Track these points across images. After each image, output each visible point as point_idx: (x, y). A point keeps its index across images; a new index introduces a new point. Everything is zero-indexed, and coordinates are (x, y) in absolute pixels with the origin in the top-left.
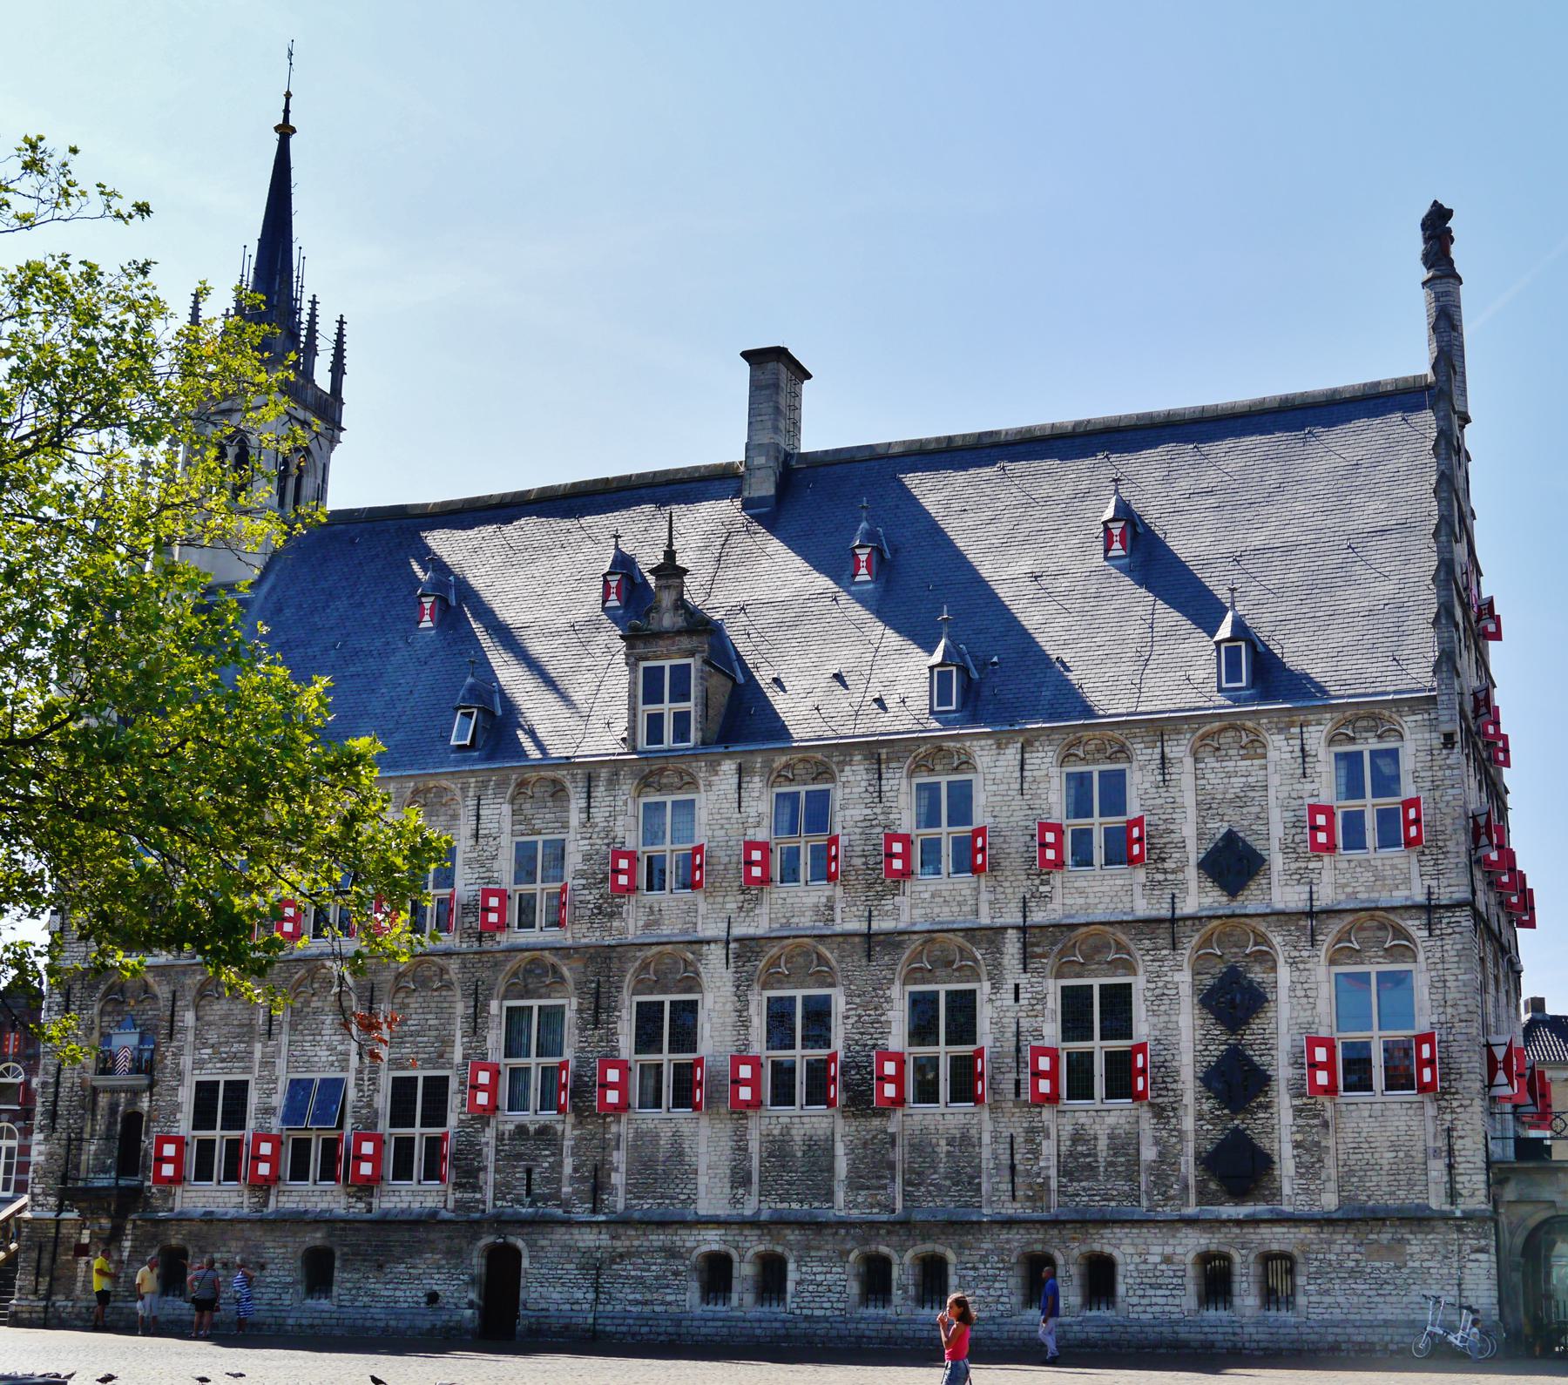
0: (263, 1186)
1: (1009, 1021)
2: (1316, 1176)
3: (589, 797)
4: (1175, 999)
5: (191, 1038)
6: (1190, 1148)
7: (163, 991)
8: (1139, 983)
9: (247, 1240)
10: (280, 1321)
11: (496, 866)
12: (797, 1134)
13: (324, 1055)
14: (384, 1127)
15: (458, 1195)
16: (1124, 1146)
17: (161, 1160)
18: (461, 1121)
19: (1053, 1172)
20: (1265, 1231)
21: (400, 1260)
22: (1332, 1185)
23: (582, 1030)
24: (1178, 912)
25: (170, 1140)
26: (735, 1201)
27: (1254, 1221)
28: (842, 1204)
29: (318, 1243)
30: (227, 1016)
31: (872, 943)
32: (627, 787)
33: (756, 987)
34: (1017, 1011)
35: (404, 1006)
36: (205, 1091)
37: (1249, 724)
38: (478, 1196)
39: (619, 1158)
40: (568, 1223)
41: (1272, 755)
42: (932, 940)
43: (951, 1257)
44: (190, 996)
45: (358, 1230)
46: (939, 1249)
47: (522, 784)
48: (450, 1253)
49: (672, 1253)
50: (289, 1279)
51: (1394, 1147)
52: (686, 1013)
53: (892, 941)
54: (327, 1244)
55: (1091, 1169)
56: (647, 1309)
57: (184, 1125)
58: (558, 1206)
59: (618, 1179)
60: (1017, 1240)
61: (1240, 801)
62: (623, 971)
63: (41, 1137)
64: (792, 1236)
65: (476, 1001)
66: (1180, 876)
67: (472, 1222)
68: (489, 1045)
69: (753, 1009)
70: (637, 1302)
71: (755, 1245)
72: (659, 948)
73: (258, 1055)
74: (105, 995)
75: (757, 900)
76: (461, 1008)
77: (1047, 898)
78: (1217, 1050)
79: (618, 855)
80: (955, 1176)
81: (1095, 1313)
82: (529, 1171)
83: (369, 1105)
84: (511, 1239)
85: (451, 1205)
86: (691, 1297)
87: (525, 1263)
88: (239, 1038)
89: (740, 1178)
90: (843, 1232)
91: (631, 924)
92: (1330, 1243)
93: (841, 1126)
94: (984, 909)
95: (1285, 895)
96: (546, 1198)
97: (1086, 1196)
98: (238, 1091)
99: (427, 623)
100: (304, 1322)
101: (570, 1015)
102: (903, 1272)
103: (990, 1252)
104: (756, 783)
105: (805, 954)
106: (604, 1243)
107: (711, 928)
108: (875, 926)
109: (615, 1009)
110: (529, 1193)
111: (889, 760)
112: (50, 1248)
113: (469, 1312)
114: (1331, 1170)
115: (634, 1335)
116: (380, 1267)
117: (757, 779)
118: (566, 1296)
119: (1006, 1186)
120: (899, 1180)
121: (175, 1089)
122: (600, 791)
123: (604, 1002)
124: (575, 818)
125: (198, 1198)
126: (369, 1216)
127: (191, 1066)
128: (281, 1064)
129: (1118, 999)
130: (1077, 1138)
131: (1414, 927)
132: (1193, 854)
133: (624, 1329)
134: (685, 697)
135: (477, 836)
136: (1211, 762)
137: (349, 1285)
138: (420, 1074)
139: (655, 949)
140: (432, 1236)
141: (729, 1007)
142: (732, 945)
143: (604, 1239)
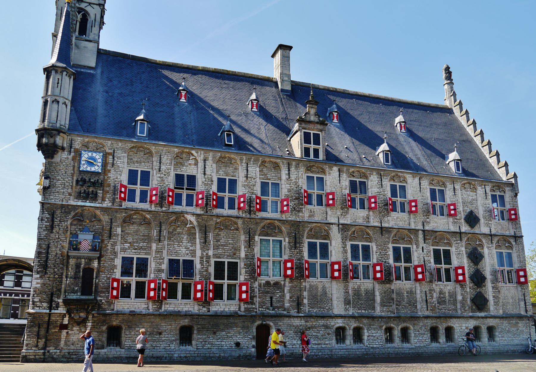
1: (422, 257)
3: (289, 170)
4: (462, 255)
5: (120, 239)
7: (105, 218)
9: (152, 322)
10: (170, 355)
11: (255, 189)
12: (362, 288)
13: (184, 250)
14: (212, 279)
16: (453, 295)
18: (245, 279)
21: (223, 330)
23: (290, 249)
26: (346, 310)
27: (486, 317)
28: (378, 311)
29: (186, 324)
31: (382, 230)
32: (302, 169)
34: (421, 254)
35: (218, 235)
36: (127, 262)
37: (473, 183)
38: (254, 306)
39: (305, 294)
40: (289, 317)
41: (478, 192)
42: (399, 231)
43: (411, 327)
44: (119, 222)
46: (408, 325)
47: (264, 162)
48: (243, 327)
49: (327, 327)
50: (173, 339)
51: (512, 298)
53: (388, 230)
55: (444, 301)
56: (320, 346)
58: (284, 310)
59: (305, 301)
60: (429, 323)
61: (471, 203)
62: (304, 231)
64: (365, 321)
65: (250, 235)
67: (252, 316)
68: (255, 251)
69: (347, 248)
70: (316, 344)
71: (354, 324)
72: (316, 224)
74: (74, 217)
75: (347, 213)
76: (243, 237)
77: (429, 223)
78: (472, 270)
80: (409, 303)
82: (271, 298)
84: (268, 322)
85: (242, 309)
86: (333, 342)
88: (144, 241)
89: (347, 302)
90: (380, 320)
91: (305, 215)
92: (503, 323)
93: (377, 286)
95: (485, 230)
96: (278, 308)
99: (183, 100)
100: (182, 355)
102: (397, 333)
104: (344, 176)
106: (303, 324)
107: (332, 219)
109: (302, 243)
110: (271, 305)
111: (384, 176)
112: (45, 326)
113: (253, 350)
115: (316, 355)
116: (215, 333)
117: (345, 174)
118: (290, 342)
119: (425, 306)
122: (293, 169)
123: (298, 240)
124: (284, 176)
125: (124, 305)
126: (209, 313)
127: (120, 250)
128: (165, 252)
130: (441, 292)
133: (313, 354)
135: (247, 177)
136: (464, 191)
137: (201, 340)
138: (226, 261)
139: (315, 224)
140: (236, 321)
141: (340, 246)
142: (340, 226)
143: (303, 322)
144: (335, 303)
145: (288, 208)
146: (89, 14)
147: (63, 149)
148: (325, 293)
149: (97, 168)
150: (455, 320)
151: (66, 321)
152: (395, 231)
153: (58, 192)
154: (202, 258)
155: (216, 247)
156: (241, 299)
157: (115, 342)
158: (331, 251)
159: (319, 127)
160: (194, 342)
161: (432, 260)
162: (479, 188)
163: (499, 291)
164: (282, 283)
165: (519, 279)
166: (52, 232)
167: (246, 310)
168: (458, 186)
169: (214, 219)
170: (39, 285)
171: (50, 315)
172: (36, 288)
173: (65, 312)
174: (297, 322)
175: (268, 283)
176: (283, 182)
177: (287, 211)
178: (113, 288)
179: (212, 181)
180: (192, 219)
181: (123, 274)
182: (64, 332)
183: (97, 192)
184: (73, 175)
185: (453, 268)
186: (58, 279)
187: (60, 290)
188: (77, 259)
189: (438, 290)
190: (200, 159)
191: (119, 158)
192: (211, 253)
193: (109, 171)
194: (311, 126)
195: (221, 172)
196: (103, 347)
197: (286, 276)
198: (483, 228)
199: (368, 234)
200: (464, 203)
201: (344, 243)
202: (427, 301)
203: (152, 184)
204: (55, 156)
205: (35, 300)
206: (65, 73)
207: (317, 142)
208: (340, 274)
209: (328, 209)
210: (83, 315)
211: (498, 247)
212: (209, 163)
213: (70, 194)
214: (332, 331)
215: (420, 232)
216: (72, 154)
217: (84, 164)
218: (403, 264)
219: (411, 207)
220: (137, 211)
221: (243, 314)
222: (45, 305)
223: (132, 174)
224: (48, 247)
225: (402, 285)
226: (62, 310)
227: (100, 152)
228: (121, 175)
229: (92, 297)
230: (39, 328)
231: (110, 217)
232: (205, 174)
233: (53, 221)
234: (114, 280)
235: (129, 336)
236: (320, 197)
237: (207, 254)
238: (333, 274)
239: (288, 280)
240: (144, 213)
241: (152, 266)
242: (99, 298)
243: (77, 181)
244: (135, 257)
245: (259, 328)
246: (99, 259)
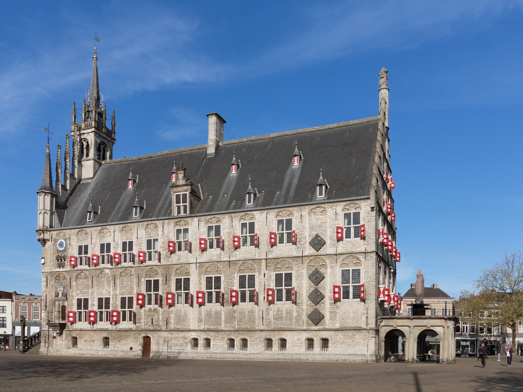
1: (263, 282)
2: (335, 319)
5: (75, 288)
6: (305, 313)
8: (294, 273)
12: (213, 310)
14: (119, 309)
16: (289, 313)
17: (69, 317)
19: (272, 319)
20: (322, 332)
21: (123, 340)
22: (338, 322)
23: (163, 285)
24: (304, 255)
25: (71, 312)
27: (319, 330)
28: (223, 327)
33: (203, 274)
35: (123, 280)
36: (79, 300)
39: (172, 316)
42: (245, 263)
43: (248, 339)
48: (134, 338)
49: (184, 338)
52: (187, 280)
55: (282, 318)
57: (75, 309)
66: (304, 246)
68: (142, 289)
69: (202, 280)
73: (90, 292)
76: (135, 280)
78: (312, 289)
79: (169, 242)
81: (282, 352)
87: (152, 340)
88: (86, 288)
89: (200, 321)
92: (337, 335)
94: (257, 255)
97: (280, 324)
98: (86, 300)
101: (160, 282)
104: (202, 224)
108: (231, 259)
111: (234, 217)
113: (139, 352)
114: (338, 318)
120: (236, 321)
122: (165, 226)
124: (160, 233)
127: (75, 295)
128: (95, 294)
129: (289, 277)
131: (361, 257)
132: (308, 240)
134: (186, 202)
141: (197, 279)
142: (198, 264)
148: (186, 315)
150: (287, 332)
154: (113, 296)
155: (121, 288)
163: (337, 307)
175: (150, 309)
190: (112, 231)
192: (118, 292)
201: (200, 277)
202: (263, 318)
215: (264, 261)
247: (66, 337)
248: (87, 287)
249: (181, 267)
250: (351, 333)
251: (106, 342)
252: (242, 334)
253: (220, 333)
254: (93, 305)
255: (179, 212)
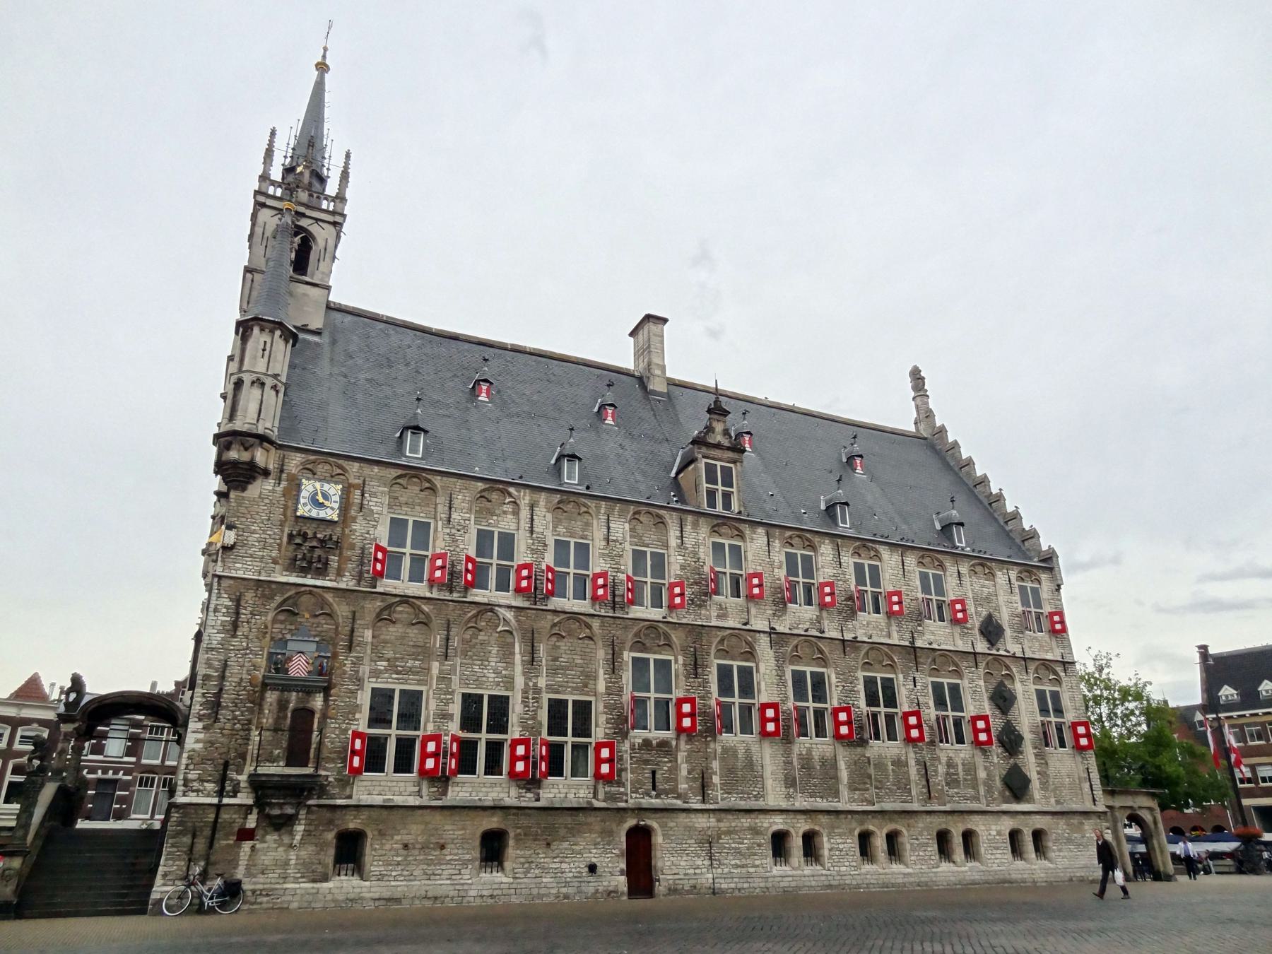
0: (439, 779)
7: (342, 610)
10: (462, 893)
12: (816, 754)
15: (607, 789)
21: (564, 839)
23: (687, 677)
26: (788, 796)
30: (403, 638)
31: (846, 645)
32: (704, 529)
35: (556, 647)
36: (381, 699)
38: (622, 790)
39: (715, 765)
41: (998, 580)
45: (529, 815)
46: (899, 827)
49: (755, 831)
50: (468, 857)
54: (502, 826)
56: (744, 870)
61: (988, 599)
63: (200, 725)
64: (824, 819)
67: (619, 810)
70: (737, 866)
71: (803, 825)
76: (602, 654)
82: (654, 773)
83: (534, 718)
84: (649, 822)
85: (601, 795)
89: (790, 782)
94: (895, 635)
96: (667, 792)
100: (485, 893)
102: (880, 843)
103: (923, 829)
104: (777, 544)
105: (812, 645)
107: (759, 624)
110: (654, 789)
112: (208, 832)
116: (548, 845)
121: (354, 692)
122: (688, 528)
124: (673, 542)
127: (367, 677)
128: (456, 679)
130: (950, 764)
133: (733, 886)
135: (608, 540)
138: (570, 698)
143: (713, 821)
144: (769, 783)
145: (683, 600)
146: (314, 239)
147: (266, 473)
148: (750, 764)
149: (331, 513)
150: (976, 818)
151: (251, 822)
152: (867, 647)
153: (251, 556)
154: (525, 692)
155: (553, 672)
156: (598, 776)
157: (351, 866)
158: (759, 684)
159: (730, 455)
160: (508, 865)
161: (932, 703)
162: (999, 573)
164: (674, 743)
165: (1077, 741)
166: (234, 636)
167: (610, 797)
168: (964, 570)
169: (550, 617)
170: (201, 745)
171: (218, 807)
172: (193, 750)
173: (250, 802)
174: (702, 822)
175: (647, 743)
176: (672, 551)
177: (681, 606)
178: (354, 753)
179: (546, 545)
180: (509, 615)
181: (373, 722)
182: (247, 845)
183: (327, 559)
184: (282, 524)
185: (968, 718)
186: (241, 733)
187: (243, 756)
188: (282, 691)
189: (944, 760)
191: (374, 495)
192: (542, 682)
193: (354, 519)
194: (717, 453)
195: (561, 529)
196: (325, 879)
197: (680, 730)
198: (1010, 645)
199: (821, 652)
200: (975, 600)
201: (780, 668)
203: (434, 547)
204: (250, 487)
205: (190, 776)
206: (278, 333)
207: (728, 482)
208: (777, 727)
209: (751, 606)
210: (289, 810)
211: (1038, 680)
212: (540, 511)
213: (275, 562)
214: (766, 840)
216: (284, 484)
217: (305, 504)
218: (882, 710)
219: (891, 603)
220: (405, 599)
221: (603, 805)
222: (210, 786)
223: (398, 526)
224: (225, 665)
225: (884, 749)
226: (244, 798)
227: (336, 483)
228: (375, 527)
229: (309, 770)
230: (194, 836)
231: (352, 608)
232: (532, 532)
233: (237, 613)
234: (357, 735)
235: (380, 852)
236: (735, 580)
237: (535, 684)
238: (763, 726)
239: (683, 737)
240: (418, 602)
241: (429, 707)
242: (323, 773)
243: (291, 536)
244: (398, 688)
245: (632, 833)
246: (326, 691)
247: (307, 833)
248: (424, 653)
249: (732, 635)
250: (1075, 820)
251: (492, 849)
252: (891, 820)
253: (843, 816)
254: (447, 717)
255: (712, 503)
